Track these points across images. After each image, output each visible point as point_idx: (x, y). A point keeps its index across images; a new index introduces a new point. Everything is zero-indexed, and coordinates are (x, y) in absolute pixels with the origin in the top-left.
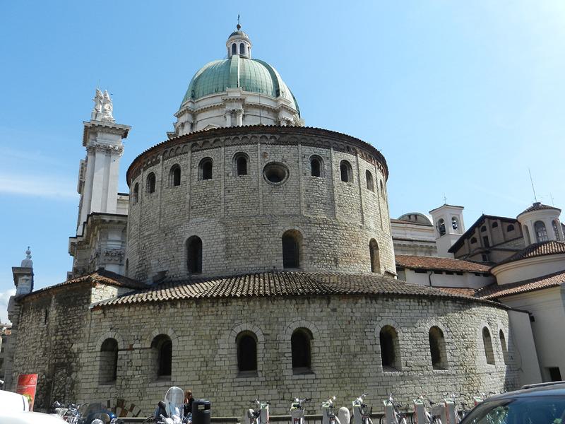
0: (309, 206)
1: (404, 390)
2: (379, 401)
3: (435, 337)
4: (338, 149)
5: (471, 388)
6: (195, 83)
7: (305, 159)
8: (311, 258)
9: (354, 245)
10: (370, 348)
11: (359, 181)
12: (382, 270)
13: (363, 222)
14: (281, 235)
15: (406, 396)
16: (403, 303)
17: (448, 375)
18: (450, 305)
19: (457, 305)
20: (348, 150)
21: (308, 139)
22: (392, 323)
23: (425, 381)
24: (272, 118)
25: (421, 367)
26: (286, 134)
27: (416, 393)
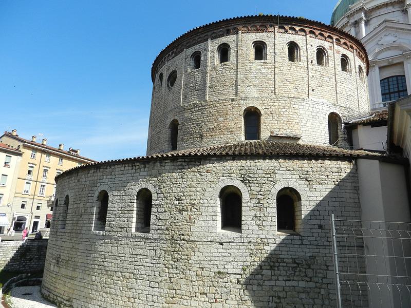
0: (186, 97)
1: (103, 249)
2: (85, 255)
3: (145, 198)
4: (213, 38)
5: (176, 256)
6: (334, 14)
7: (187, 59)
9: (221, 119)
11: (237, 57)
12: (265, 135)
13: (236, 94)
14: (168, 126)
15: (103, 253)
16: (118, 169)
18: (168, 165)
20: (228, 33)
22: (106, 188)
23: (122, 243)
24: (399, 9)
25: (122, 228)
26: (178, 45)
27: (111, 253)
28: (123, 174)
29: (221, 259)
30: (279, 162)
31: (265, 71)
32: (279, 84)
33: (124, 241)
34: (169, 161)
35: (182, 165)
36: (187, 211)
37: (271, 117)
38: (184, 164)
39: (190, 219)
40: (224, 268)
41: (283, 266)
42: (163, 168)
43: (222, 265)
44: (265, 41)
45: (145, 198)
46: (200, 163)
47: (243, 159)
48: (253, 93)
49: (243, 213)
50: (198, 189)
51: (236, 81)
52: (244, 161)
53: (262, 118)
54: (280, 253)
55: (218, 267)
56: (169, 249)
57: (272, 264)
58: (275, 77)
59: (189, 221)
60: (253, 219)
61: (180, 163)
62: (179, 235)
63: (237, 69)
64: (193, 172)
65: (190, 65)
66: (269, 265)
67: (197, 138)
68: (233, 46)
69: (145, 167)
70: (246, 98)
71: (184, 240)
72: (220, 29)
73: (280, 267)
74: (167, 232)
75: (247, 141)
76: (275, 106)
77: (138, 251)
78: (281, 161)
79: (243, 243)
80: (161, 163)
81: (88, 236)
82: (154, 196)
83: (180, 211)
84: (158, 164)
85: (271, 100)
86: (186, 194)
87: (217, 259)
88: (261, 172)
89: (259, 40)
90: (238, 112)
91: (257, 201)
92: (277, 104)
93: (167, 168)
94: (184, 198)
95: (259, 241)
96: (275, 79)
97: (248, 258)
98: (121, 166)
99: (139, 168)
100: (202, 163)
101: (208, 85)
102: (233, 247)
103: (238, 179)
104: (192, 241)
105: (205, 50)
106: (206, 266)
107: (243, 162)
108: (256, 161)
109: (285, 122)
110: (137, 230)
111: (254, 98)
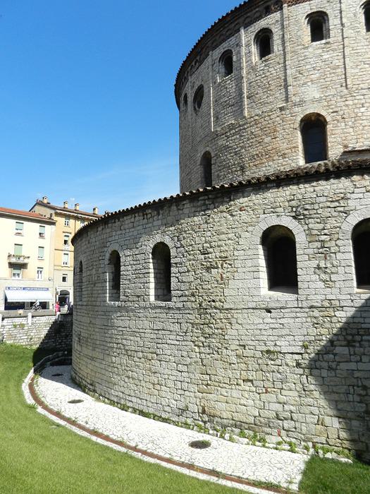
0: (217, 118)
1: (121, 323)
4: (246, 26)
5: (207, 330)
8: (218, 176)
9: (267, 140)
12: (334, 151)
13: (287, 100)
14: (199, 162)
15: (120, 329)
16: (128, 220)
17: (169, 308)
18: (187, 205)
21: (217, 37)
22: (115, 247)
25: (138, 296)
28: (134, 227)
29: (270, 332)
30: (352, 181)
31: (328, 56)
32: (353, 71)
33: (142, 313)
34: (187, 201)
35: (204, 204)
36: (217, 268)
37: (343, 124)
38: (207, 202)
39: (222, 278)
40: (276, 345)
42: (181, 212)
43: (272, 341)
44: (325, 10)
45: (161, 253)
46: (230, 198)
47: (293, 184)
48: (312, 92)
49: (299, 265)
50: (230, 236)
51: (285, 80)
52: (295, 187)
53: (329, 127)
54: (362, 320)
55: (265, 344)
56: (197, 321)
57: (350, 338)
58: (344, 62)
59: (220, 282)
60: (315, 273)
61: (202, 202)
62: (209, 302)
63: (285, 62)
64: (222, 212)
65: (218, 72)
66: (345, 339)
67: (237, 171)
68: (276, 31)
69: (158, 214)
70: (301, 103)
71: (216, 308)
72: (254, 9)
74: (193, 299)
75: (308, 165)
76: (347, 105)
77: (160, 326)
78: (355, 178)
79: (301, 308)
80: (177, 206)
81: (104, 309)
82: (173, 252)
83: (208, 269)
84: (174, 208)
85: (341, 97)
86: (213, 244)
87: (264, 332)
88: (322, 199)
89: (315, 10)
90: (292, 126)
91: (319, 244)
92: (351, 103)
93: (186, 211)
94: (211, 250)
96: (345, 64)
97: (310, 331)
100: (232, 198)
101: (245, 95)
102: (287, 315)
103: (288, 214)
104: (227, 309)
105: (237, 45)
106: (250, 343)
107: (293, 189)
108: (314, 184)
109: (366, 128)
110: (157, 297)
111: (313, 101)
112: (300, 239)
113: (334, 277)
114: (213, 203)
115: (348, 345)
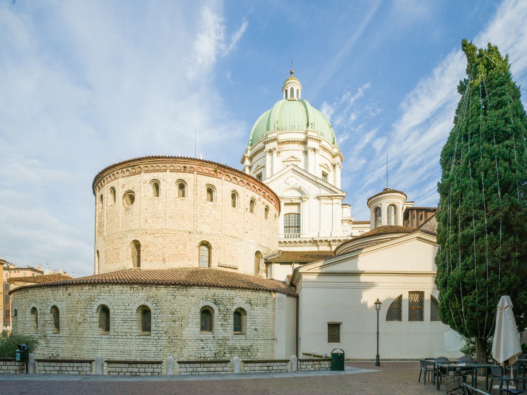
10: (89, 319)
19: (170, 289)
28: (122, 293)
34: (163, 286)
35: (173, 290)
38: (175, 289)
41: (236, 351)
42: (159, 291)
46: (187, 290)
57: (231, 350)
60: (221, 326)
61: (172, 289)
66: (229, 351)
69: (143, 289)
73: (234, 352)
82: (153, 311)
95: (224, 338)
97: (218, 348)
98: (119, 286)
99: (137, 290)
100: (188, 290)
112: (216, 312)
113: (227, 328)
114: (178, 290)
115: (230, 353)
